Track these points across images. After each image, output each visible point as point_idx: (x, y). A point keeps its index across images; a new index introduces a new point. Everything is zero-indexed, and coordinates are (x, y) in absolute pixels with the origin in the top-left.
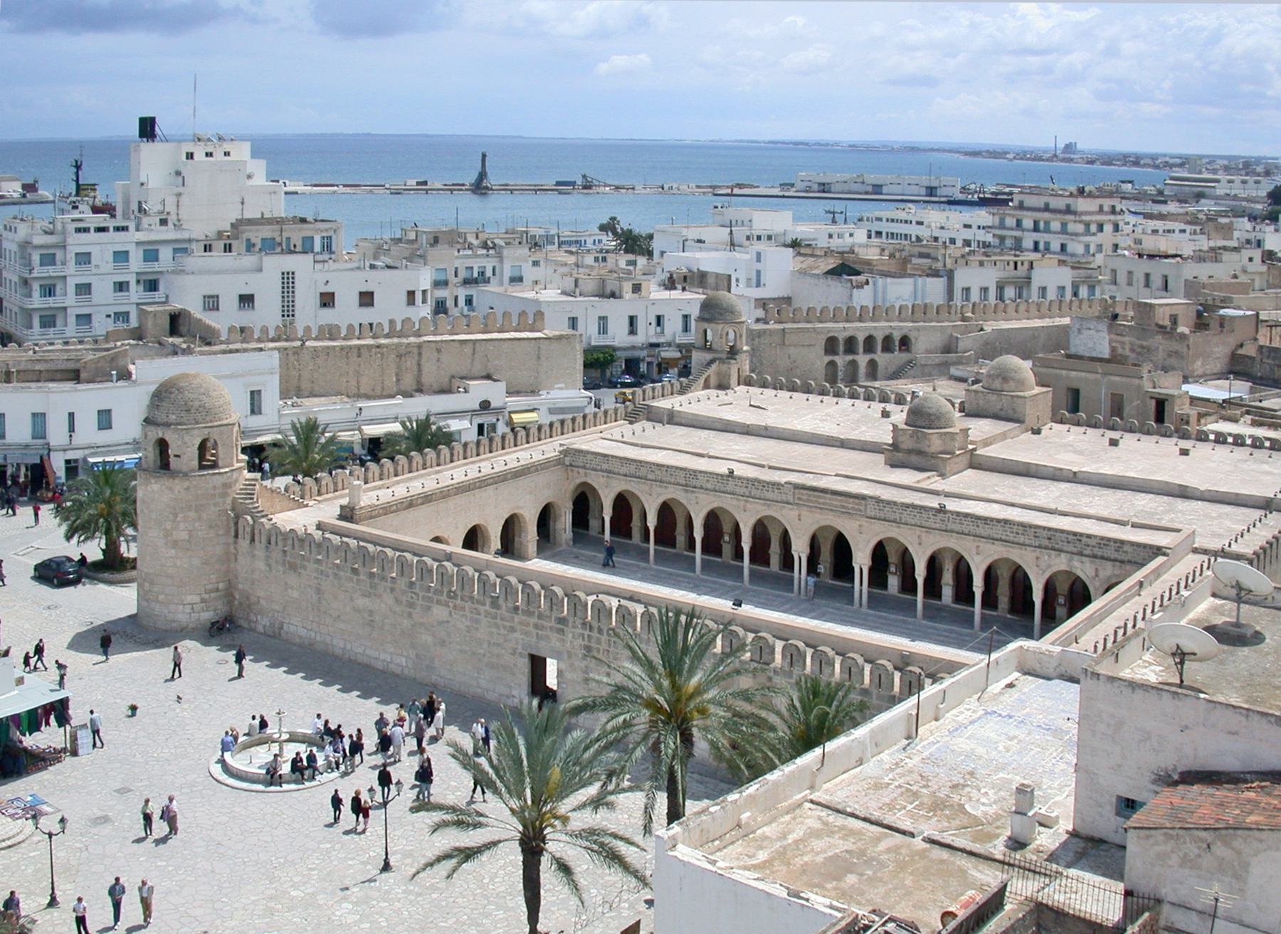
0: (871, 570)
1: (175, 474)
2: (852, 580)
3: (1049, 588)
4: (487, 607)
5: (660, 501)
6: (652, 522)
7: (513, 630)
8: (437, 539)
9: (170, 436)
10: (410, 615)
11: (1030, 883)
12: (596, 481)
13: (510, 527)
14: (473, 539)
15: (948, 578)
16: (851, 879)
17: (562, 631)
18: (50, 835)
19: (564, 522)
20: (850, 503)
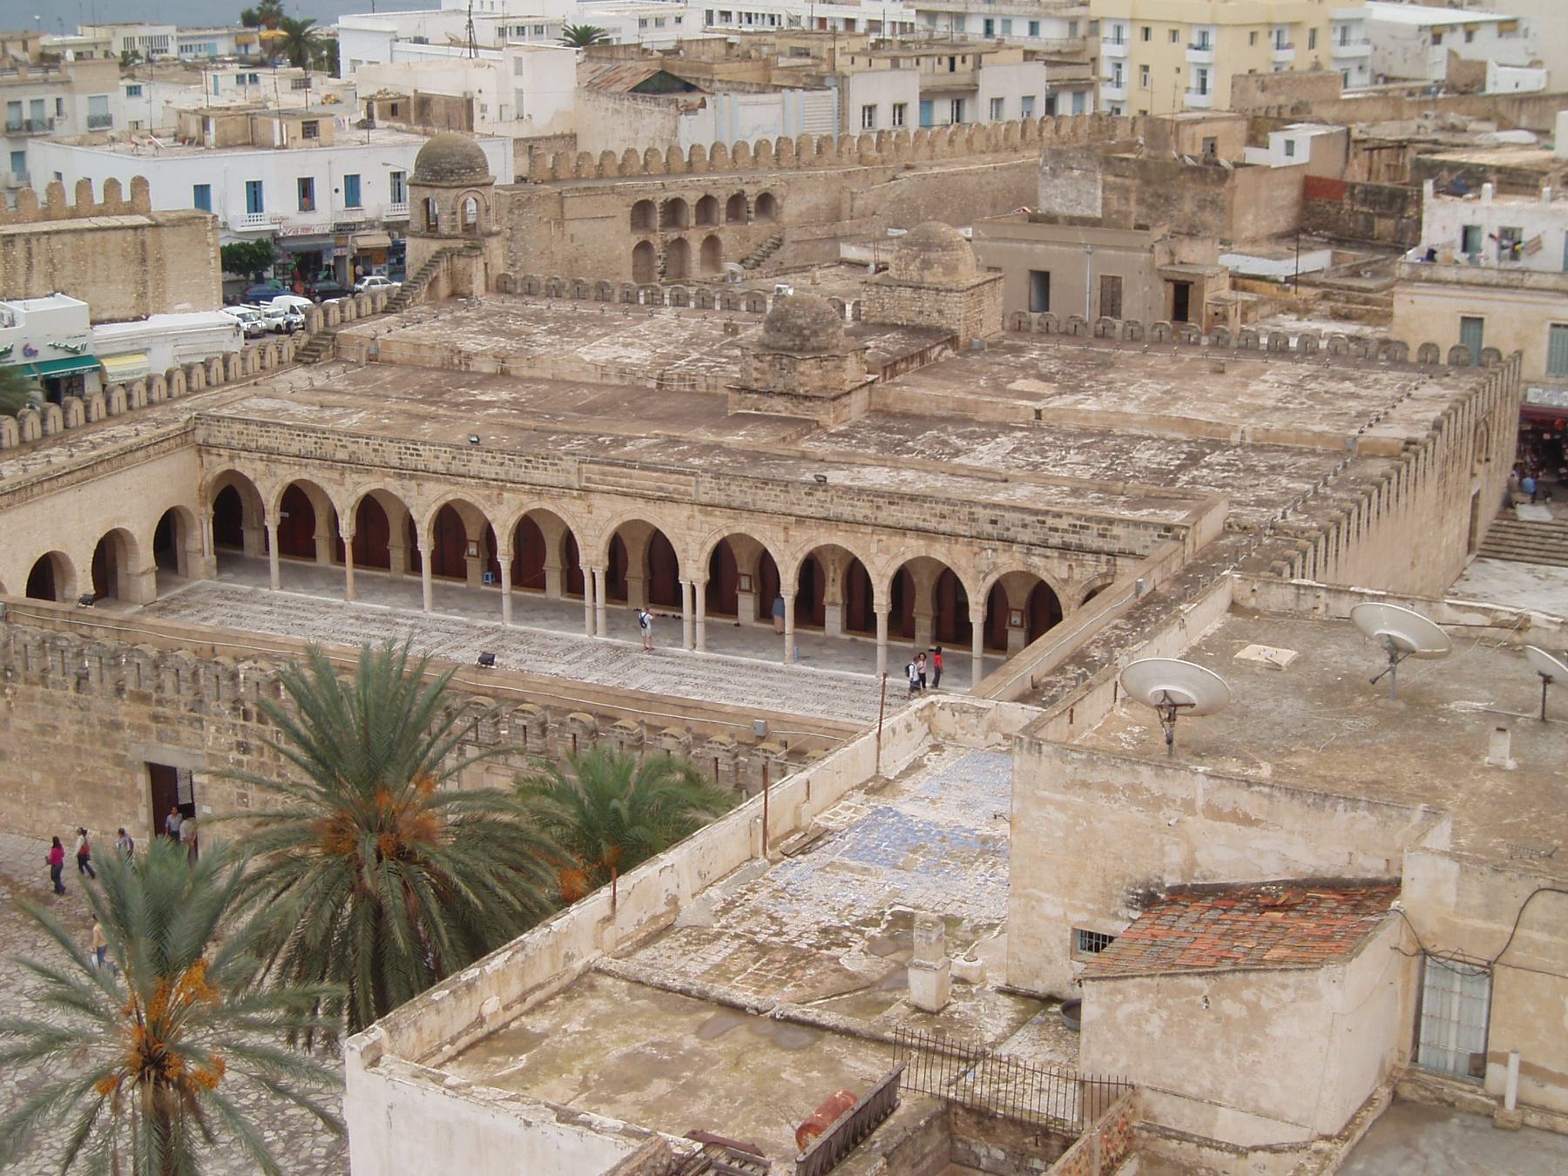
3: (996, 597)
4: (71, 693)
6: (347, 529)
11: (936, 1073)
12: (249, 468)
13: (109, 553)
15: (833, 592)
16: (660, 1087)
19: (200, 536)
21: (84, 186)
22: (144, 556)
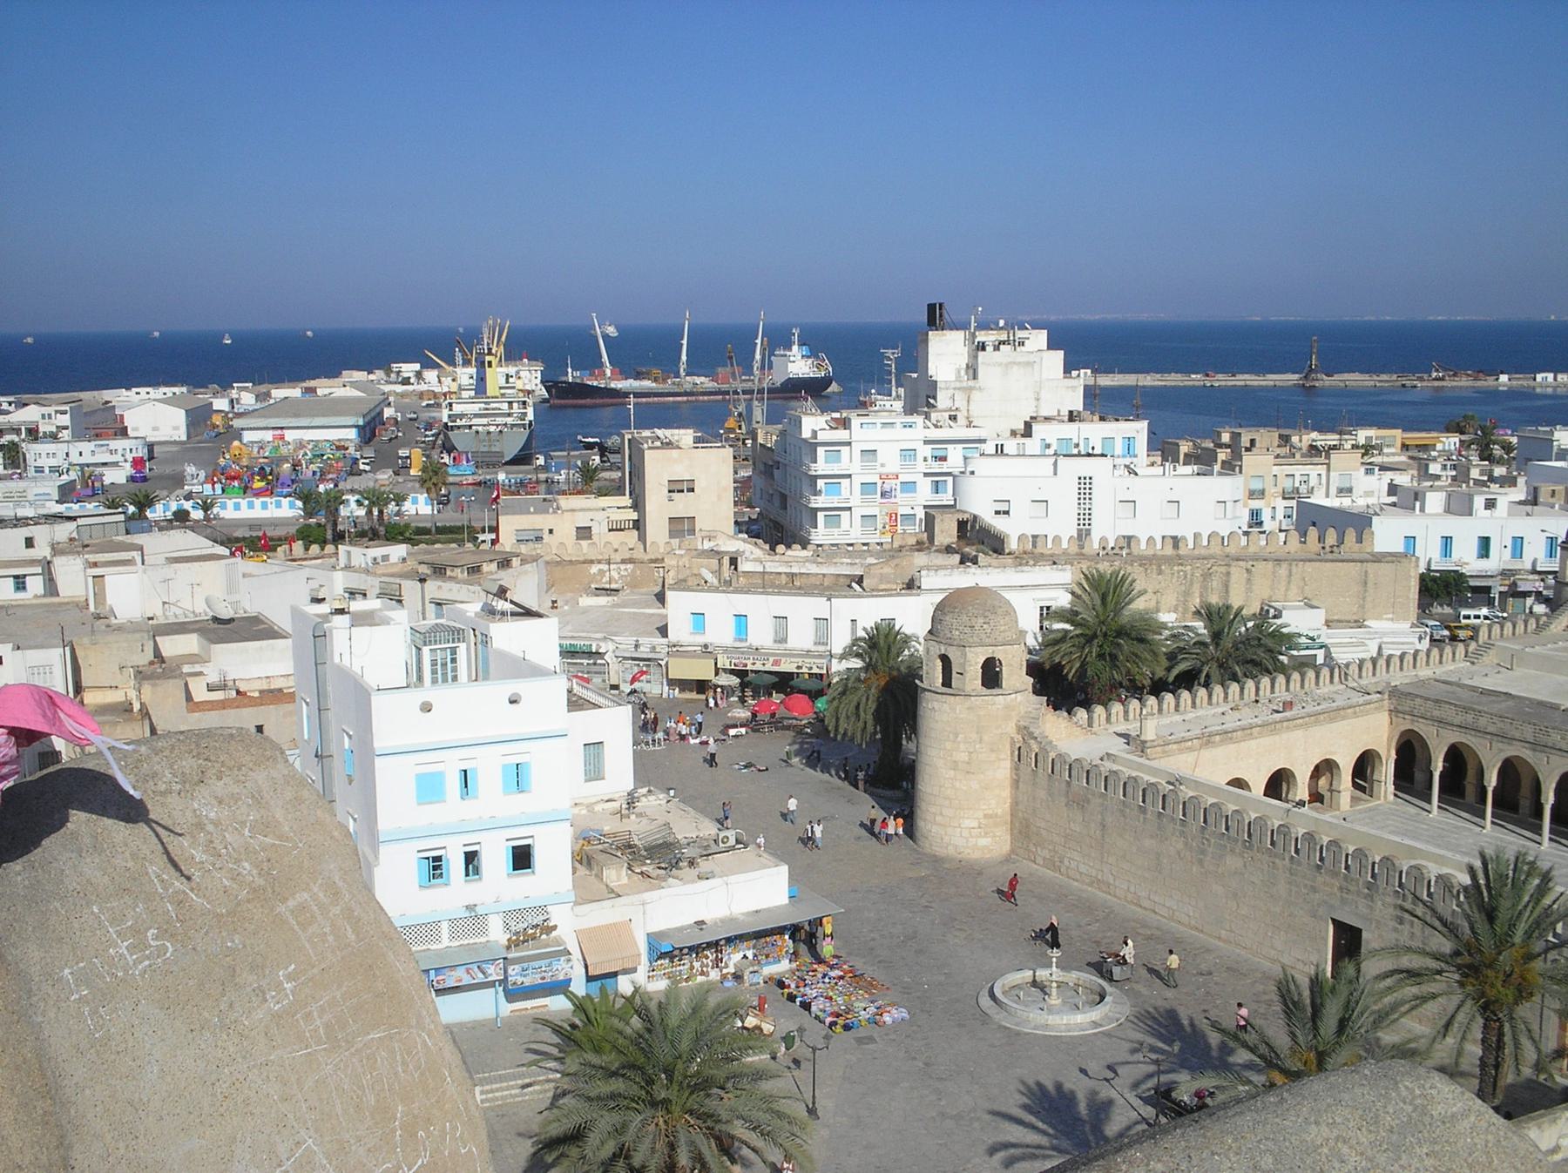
6: (1492, 780)
7: (1314, 890)
10: (1201, 862)
12: (1423, 729)
14: (1277, 784)
17: (1370, 897)
18: (814, 1050)
19: (1386, 772)
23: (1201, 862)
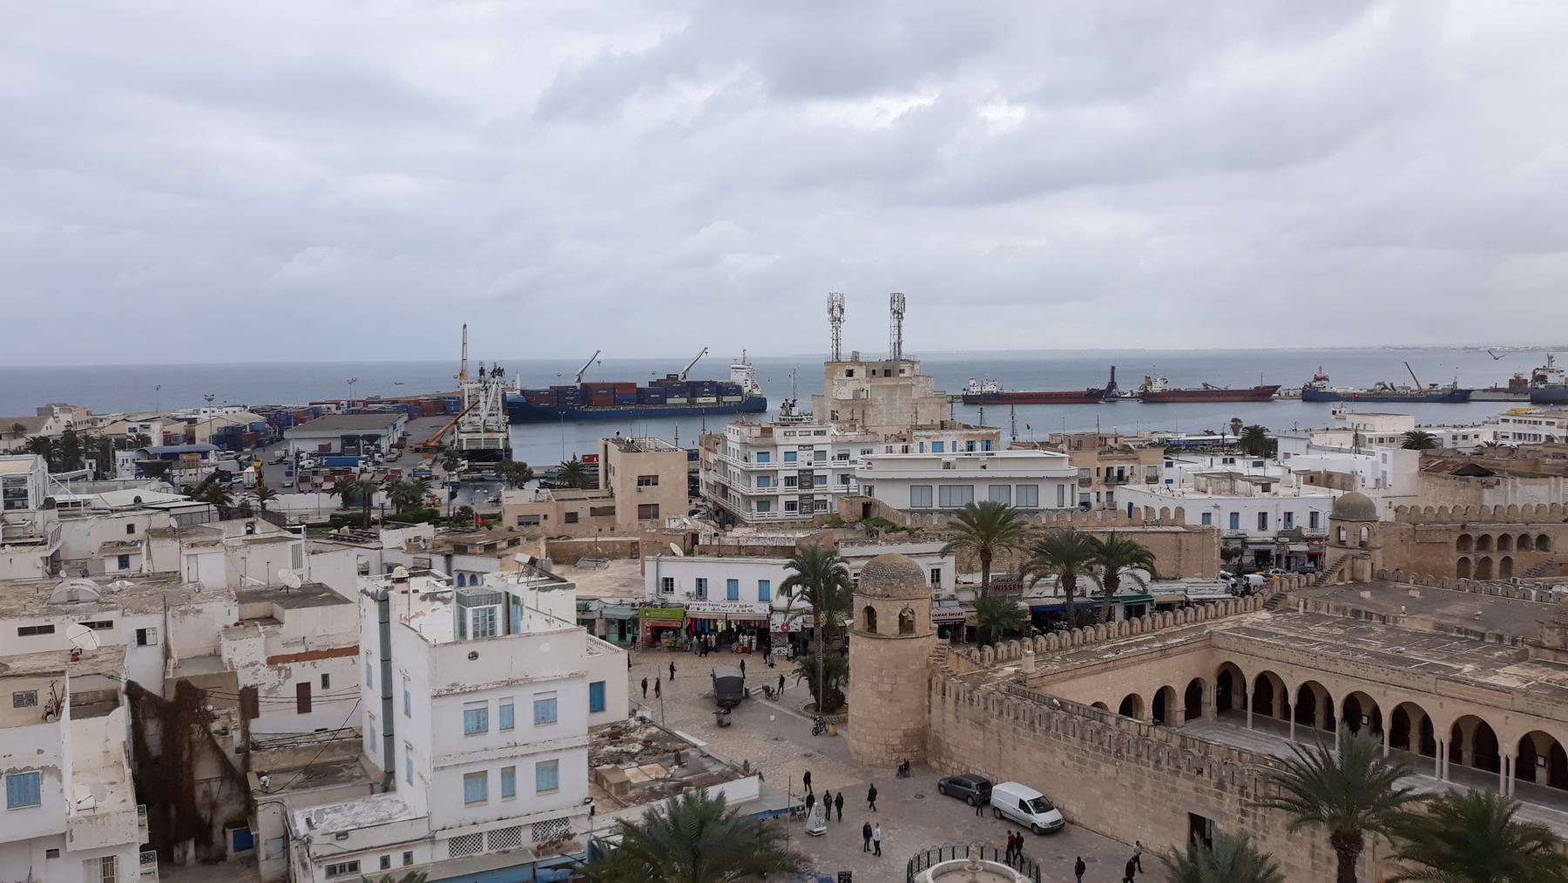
0: (1518, 760)
1: (880, 638)
2: (1498, 770)
5: (1301, 682)
6: (1292, 700)
8: (1097, 705)
9: (877, 606)
12: (1239, 661)
13: (1162, 697)
14: (1129, 706)
17: (1220, 796)
19: (1210, 696)
20: (1497, 698)
21: (1164, 510)
22: (1179, 704)
23: (1080, 770)
